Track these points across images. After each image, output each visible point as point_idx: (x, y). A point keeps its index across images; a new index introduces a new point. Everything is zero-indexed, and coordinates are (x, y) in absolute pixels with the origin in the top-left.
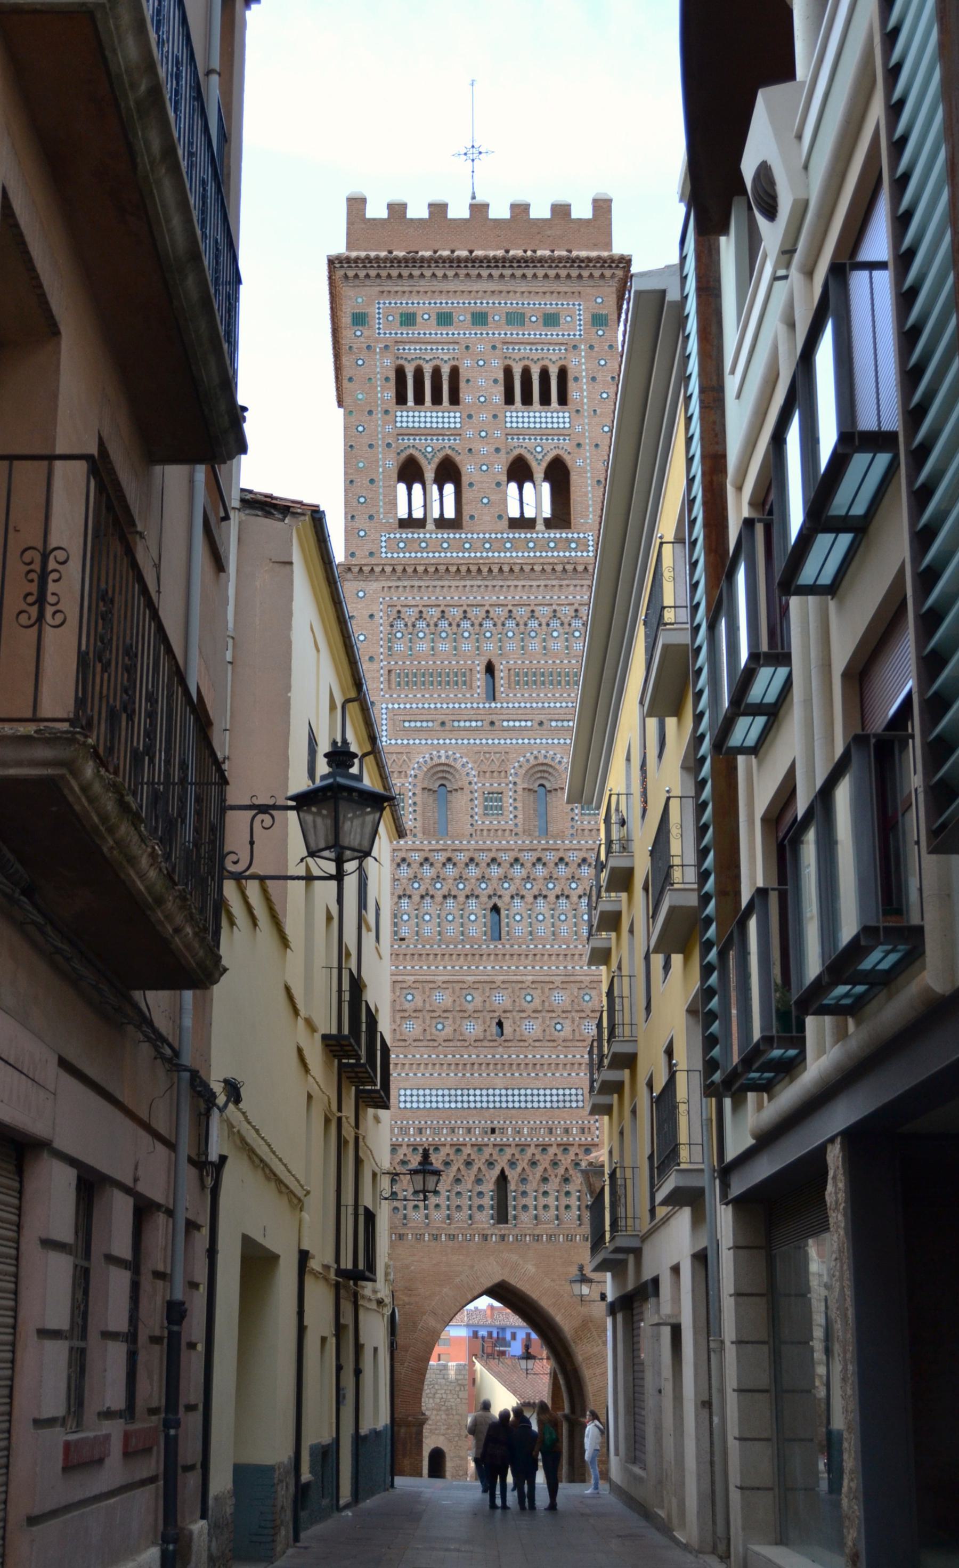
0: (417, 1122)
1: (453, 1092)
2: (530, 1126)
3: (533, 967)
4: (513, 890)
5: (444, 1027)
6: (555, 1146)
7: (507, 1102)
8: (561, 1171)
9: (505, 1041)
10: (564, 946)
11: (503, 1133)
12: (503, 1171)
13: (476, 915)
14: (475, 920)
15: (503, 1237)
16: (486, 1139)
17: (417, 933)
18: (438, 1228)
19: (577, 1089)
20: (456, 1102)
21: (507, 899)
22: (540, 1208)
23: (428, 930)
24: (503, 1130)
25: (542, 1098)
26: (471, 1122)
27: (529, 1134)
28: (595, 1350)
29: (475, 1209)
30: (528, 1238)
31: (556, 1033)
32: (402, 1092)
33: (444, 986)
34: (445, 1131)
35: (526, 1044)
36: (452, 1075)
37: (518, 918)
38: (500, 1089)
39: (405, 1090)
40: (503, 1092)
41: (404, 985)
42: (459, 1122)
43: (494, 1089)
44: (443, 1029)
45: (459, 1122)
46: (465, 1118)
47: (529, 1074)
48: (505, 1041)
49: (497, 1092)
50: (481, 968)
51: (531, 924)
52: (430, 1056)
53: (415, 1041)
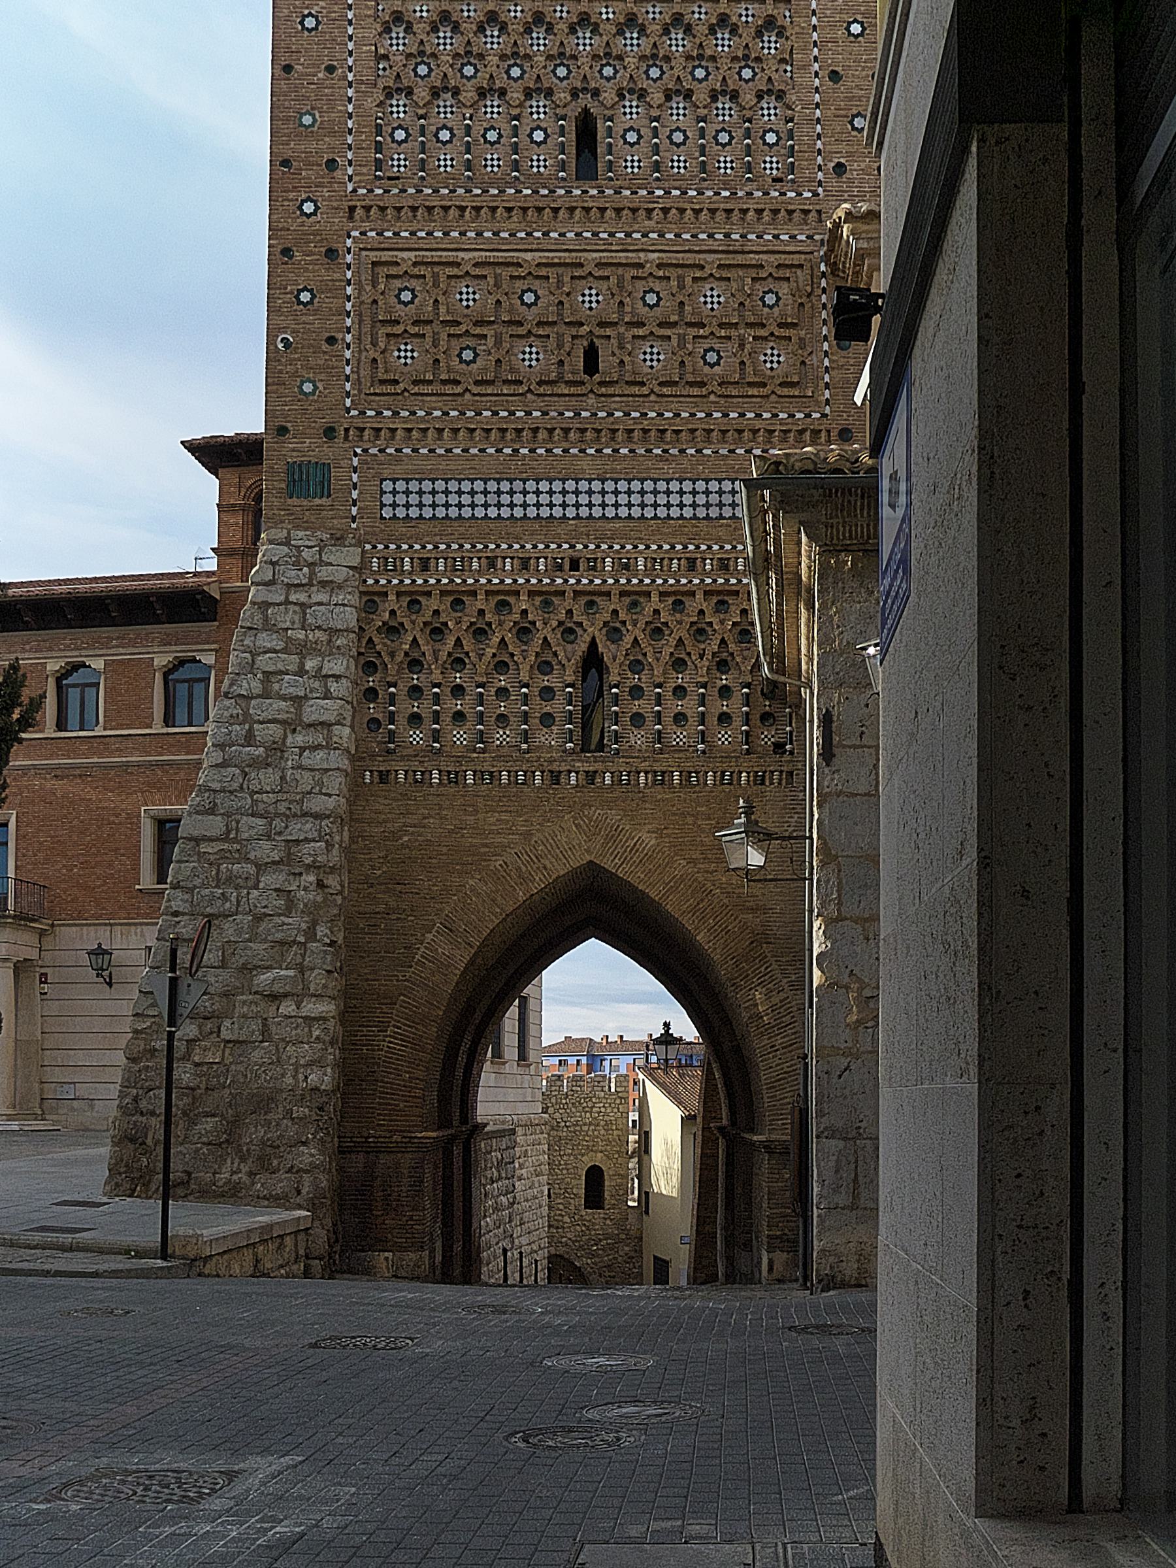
1: (492, 486)
2: (648, 553)
3: (661, 235)
4: (623, 78)
5: (476, 355)
6: (699, 596)
7: (604, 505)
9: (602, 384)
10: (726, 193)
11: (594, 568)
12: (593, 644)
13: (545, 130)
14: (544, 142)
15: (591, 776)
17: (423, 165)
18: (458, 760)
20: (499, 505)
21: (609, 96)
22: (668, 719)
23: (446, 161)
24: (594, 565)
26: (529, 546)
27: (648, 572)
30: (642, 779)
31: (707, 369)
32: (388, 486)
33: (478, 271)
34: (475, 565)
35: (645, 390)
36: (491, 451)
37: (632, 137)
38: (590, 481)
39: (394, 481)
41: (394, 271)
42: (504, 546)
43: (577, 481)
44: (474, 361)
45: (504, 546)
46: (517, 539)
47: (649, 451)
48: (602, 384)
49: (583, 486)
50: (554, 235)
51: (656, 150)
52: (446, 414)
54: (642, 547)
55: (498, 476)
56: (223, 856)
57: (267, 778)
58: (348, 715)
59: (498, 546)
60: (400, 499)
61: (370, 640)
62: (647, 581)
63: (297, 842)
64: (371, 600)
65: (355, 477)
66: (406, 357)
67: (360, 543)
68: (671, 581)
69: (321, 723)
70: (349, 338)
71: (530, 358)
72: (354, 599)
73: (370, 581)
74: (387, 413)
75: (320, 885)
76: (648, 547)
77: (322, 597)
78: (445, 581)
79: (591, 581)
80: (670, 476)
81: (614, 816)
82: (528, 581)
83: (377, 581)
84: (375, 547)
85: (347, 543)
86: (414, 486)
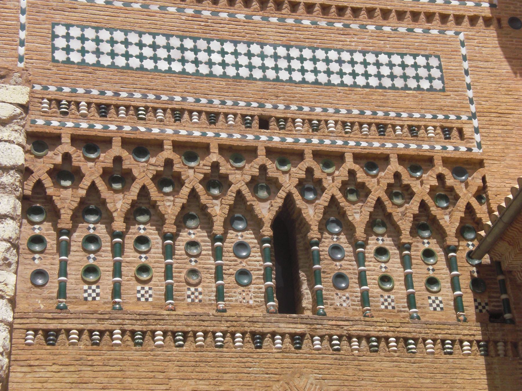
0: (95, 92)
8: (414, 207)
15: (297, 339)
16: (250, 137)
18: (143, 317)
19: (427, 57)
26: (216, 102)
29: (229, 281)
30: (355, 344)
34: (160, 114)
39: (68, 26)
40: (282, 51)
42: (191, 99)
45: (191, 99)
49: (269, 50)
54: (331, 110)
55: (180, 33)
59: (184, 99)
61: (39, 184)
62: (340, 142)
65: (23, 19)
67: (29, 82)
68: (364, 144)
72: (22, 139)
73: (40, 122)
76: (337, 111)
78: (127, 128)
79: (283, 140)
80: (352, 48)
82: (217, 135)
83: (48, 123)
84: (46, 88)
85: (12, 81)
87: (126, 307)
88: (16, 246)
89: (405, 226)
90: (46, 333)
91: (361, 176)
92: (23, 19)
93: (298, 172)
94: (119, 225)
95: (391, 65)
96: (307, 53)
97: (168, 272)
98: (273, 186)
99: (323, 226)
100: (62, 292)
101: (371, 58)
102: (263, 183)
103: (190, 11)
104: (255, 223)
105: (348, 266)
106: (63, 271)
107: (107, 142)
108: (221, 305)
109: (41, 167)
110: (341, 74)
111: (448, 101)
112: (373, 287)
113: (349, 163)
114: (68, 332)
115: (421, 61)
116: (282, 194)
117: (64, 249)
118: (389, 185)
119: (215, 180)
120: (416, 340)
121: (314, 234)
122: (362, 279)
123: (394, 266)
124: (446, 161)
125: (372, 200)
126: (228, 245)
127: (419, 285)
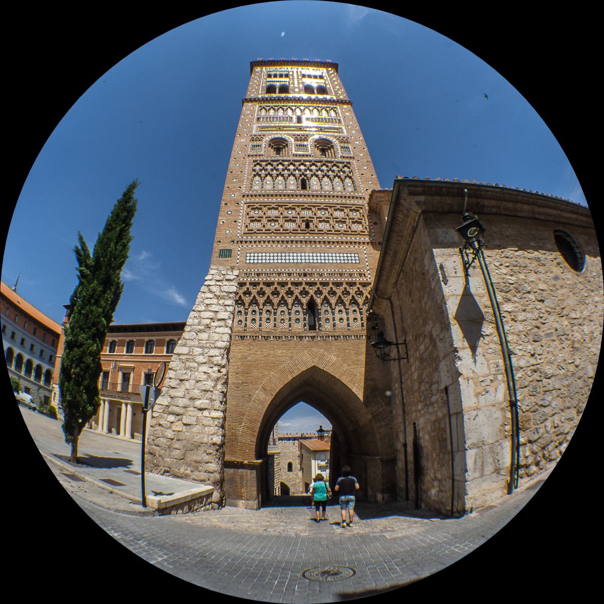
8: (350, 297)
9: (311, 231)
15: (313, 337)
25: (334, 258)
28: (381, 410)
29: (293, 322)
30: (330, 338)
31: (340, 228)
32: (248, 255)
34: (274, 275)
40: (311, 254)
46: (287, 268)
49: (307, 254)
53: (258, 230)
56: (188, 360)
57: (204, 336)
58: (232, 317)
60: (252, 258)
61: (240, 297)
63: (212, 356)
64: (241, 284)
65: (239, 253)
66: (256, 226)
67: (239, 269)
69: (223, 319)
70: (240, 221)
71: (290, 226)
72: (236, 284)
73: (241, 280)
74: (249, 237)
75: (219, 371)
77: (226, 283)
78: (265, 279)
81: (322, 351)
86: (256, 255)
87: (263, 330)
88: (233, 314)
89: (347, 303)
90: (241, 337)
91: (334, 289)
92: (239, 253)
93: (315, 288)
94: (261, 307)
95: (344, 257)
96: (319, 255)
97: (275, 320)
98: (307, 293)
99: (322, 304)
100: (246, 326)
101: (338, 255)
102: (304, 293)
103: (284, 246)
104: (302, 305)
105: (330, 316)
106: (246, 320)
107: (259, 284)
108: (290, 329)
109: (241, 292)
110: (329, 260)
111: (360, 266)
112: (337, 322)
113: (331, 285)
114: (247, 336)
115: (353, 255)
116: (310, 295)
117: (246, 314)
118: (343, 291)
119: (290, 292)
120: (349, 336)
121: (319, 307)
122: (334, 319)
123: (344, 315)
124: (360, 284)
125: (337, 296)
126: (293, 311)
127: (351, 320)
